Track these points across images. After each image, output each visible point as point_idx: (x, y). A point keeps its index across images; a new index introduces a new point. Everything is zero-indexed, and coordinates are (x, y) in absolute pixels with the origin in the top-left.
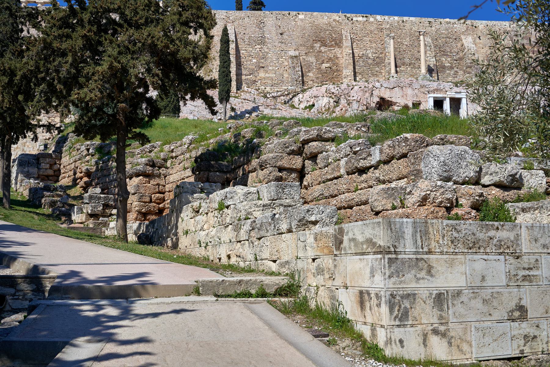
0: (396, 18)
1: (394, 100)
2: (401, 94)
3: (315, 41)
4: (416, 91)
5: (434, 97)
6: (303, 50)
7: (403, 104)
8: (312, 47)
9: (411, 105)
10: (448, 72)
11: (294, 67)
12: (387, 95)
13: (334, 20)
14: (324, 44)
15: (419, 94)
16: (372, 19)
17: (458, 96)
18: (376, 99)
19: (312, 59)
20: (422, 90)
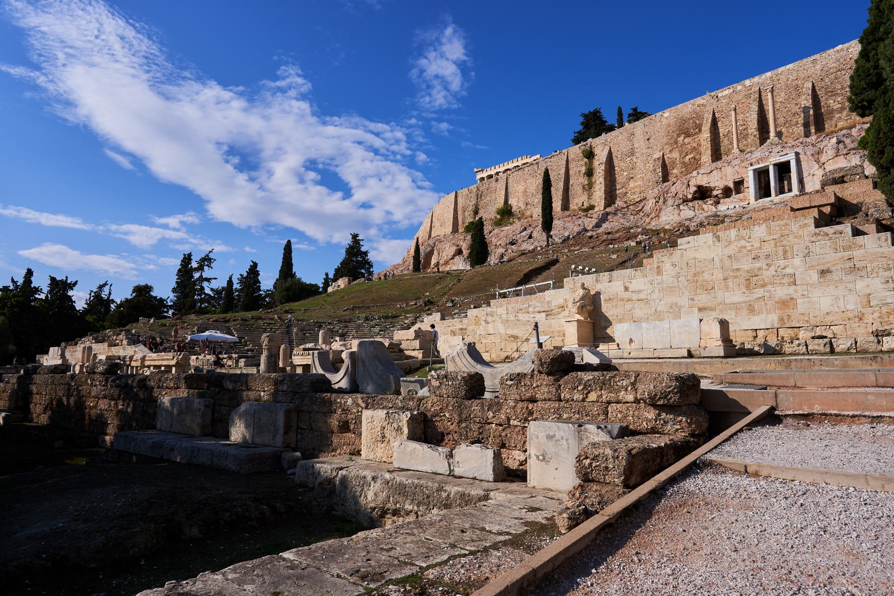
0: (769, 74)
1: (712, 185)
2: (720, 176)
3: (679, 136)
4: (737, 168)
5: (754, 170)
6: (667, 149)
7: (722, 186)
8: (676, 142)
9: (731, 185)
10: (837, 116)
11: (655, 170)
12: (703, 181)
13: (699, 106)
14: (688, 135)
15: (740, 170)
16: (739, 87)
17: (784, 159)
18: (693, 189)
19: (676, 155)
20: (743, 164)
